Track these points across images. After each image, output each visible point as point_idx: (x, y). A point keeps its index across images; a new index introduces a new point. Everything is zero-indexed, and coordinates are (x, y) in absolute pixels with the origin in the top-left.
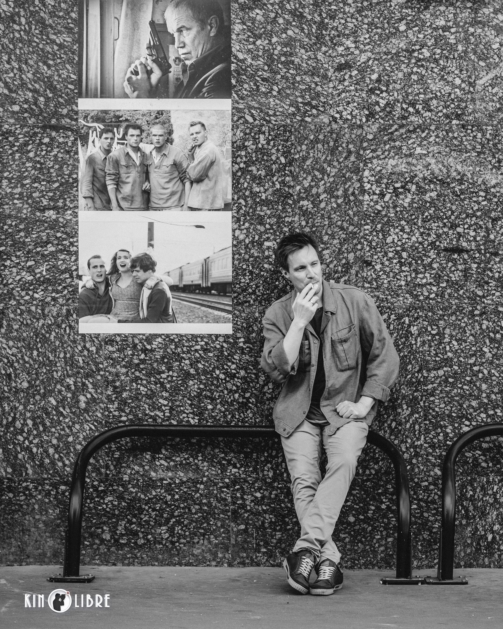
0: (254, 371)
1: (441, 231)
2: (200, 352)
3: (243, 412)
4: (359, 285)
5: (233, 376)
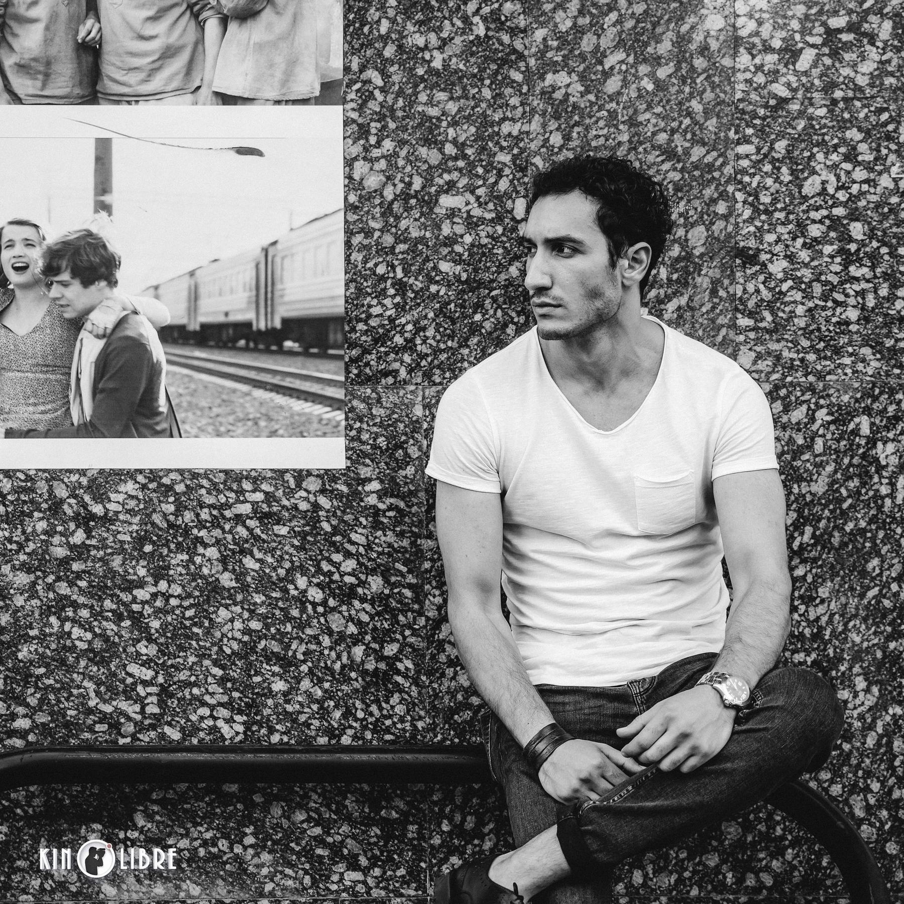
0: (411, 579)
2: (251, 523)
3: (377, 701)
4: (721, 320)
5: (348, 595)
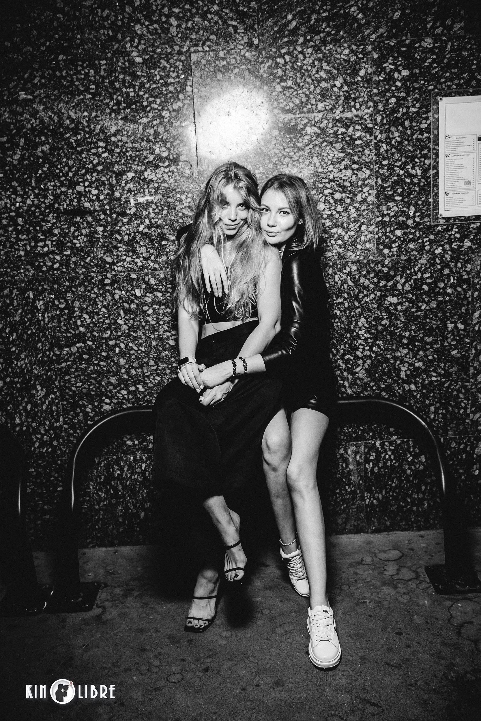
1: (58, 191)
